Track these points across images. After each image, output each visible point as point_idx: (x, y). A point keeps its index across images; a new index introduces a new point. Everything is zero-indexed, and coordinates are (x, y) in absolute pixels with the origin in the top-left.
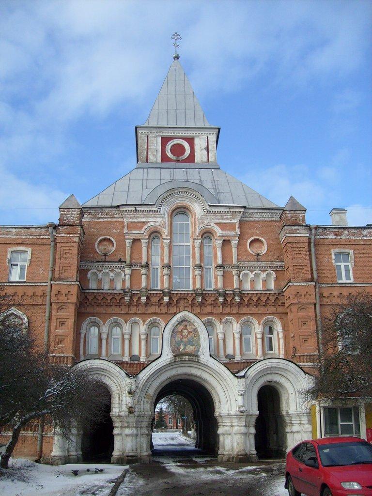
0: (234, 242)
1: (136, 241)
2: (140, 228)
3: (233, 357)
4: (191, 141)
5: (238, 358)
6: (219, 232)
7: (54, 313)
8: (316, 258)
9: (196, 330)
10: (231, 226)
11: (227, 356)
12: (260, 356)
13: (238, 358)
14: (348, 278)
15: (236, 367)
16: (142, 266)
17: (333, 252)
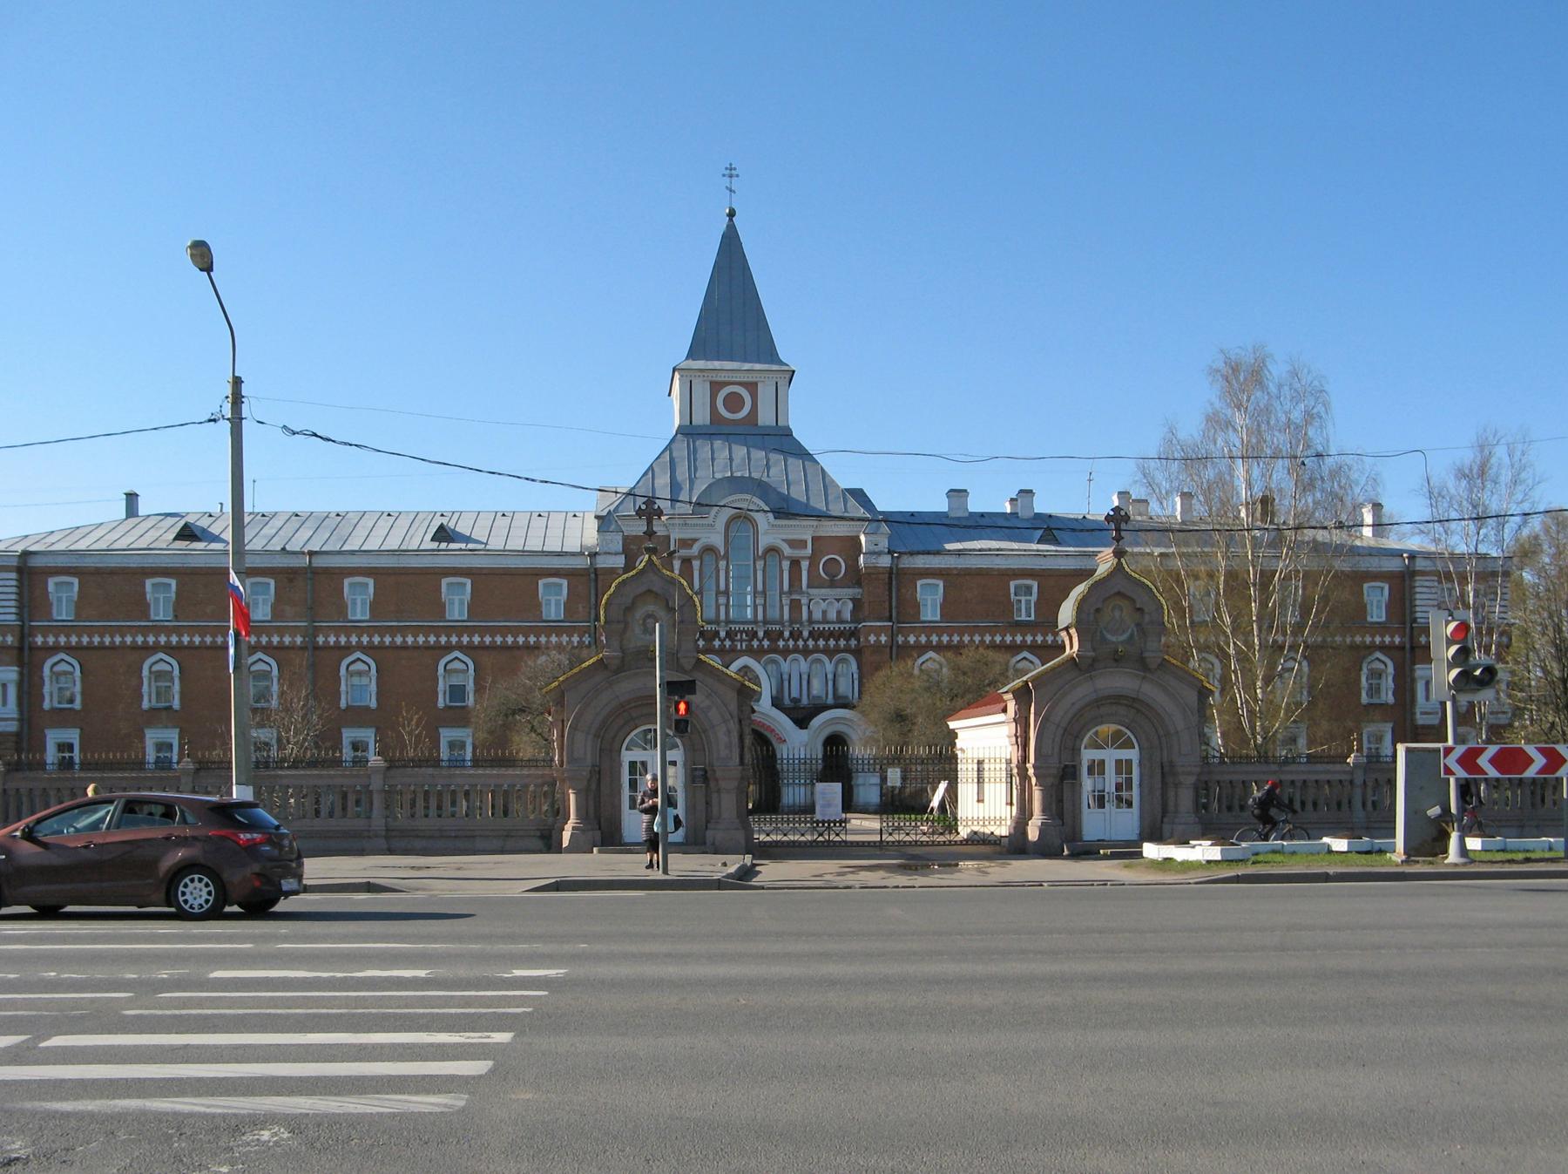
0: (805, 565)
1: (687, 562)
2: (691, 546)
3: (799, 700)
4: (752, 387)
5: (805, 701)
6: (787, 551)
8: (898, 590)
10: (803, 544)
11: (796, 701)
12: (830, 700)
13: (805, 701)
14: (934, 614)
15: (802, 717)
17: (919, 583)
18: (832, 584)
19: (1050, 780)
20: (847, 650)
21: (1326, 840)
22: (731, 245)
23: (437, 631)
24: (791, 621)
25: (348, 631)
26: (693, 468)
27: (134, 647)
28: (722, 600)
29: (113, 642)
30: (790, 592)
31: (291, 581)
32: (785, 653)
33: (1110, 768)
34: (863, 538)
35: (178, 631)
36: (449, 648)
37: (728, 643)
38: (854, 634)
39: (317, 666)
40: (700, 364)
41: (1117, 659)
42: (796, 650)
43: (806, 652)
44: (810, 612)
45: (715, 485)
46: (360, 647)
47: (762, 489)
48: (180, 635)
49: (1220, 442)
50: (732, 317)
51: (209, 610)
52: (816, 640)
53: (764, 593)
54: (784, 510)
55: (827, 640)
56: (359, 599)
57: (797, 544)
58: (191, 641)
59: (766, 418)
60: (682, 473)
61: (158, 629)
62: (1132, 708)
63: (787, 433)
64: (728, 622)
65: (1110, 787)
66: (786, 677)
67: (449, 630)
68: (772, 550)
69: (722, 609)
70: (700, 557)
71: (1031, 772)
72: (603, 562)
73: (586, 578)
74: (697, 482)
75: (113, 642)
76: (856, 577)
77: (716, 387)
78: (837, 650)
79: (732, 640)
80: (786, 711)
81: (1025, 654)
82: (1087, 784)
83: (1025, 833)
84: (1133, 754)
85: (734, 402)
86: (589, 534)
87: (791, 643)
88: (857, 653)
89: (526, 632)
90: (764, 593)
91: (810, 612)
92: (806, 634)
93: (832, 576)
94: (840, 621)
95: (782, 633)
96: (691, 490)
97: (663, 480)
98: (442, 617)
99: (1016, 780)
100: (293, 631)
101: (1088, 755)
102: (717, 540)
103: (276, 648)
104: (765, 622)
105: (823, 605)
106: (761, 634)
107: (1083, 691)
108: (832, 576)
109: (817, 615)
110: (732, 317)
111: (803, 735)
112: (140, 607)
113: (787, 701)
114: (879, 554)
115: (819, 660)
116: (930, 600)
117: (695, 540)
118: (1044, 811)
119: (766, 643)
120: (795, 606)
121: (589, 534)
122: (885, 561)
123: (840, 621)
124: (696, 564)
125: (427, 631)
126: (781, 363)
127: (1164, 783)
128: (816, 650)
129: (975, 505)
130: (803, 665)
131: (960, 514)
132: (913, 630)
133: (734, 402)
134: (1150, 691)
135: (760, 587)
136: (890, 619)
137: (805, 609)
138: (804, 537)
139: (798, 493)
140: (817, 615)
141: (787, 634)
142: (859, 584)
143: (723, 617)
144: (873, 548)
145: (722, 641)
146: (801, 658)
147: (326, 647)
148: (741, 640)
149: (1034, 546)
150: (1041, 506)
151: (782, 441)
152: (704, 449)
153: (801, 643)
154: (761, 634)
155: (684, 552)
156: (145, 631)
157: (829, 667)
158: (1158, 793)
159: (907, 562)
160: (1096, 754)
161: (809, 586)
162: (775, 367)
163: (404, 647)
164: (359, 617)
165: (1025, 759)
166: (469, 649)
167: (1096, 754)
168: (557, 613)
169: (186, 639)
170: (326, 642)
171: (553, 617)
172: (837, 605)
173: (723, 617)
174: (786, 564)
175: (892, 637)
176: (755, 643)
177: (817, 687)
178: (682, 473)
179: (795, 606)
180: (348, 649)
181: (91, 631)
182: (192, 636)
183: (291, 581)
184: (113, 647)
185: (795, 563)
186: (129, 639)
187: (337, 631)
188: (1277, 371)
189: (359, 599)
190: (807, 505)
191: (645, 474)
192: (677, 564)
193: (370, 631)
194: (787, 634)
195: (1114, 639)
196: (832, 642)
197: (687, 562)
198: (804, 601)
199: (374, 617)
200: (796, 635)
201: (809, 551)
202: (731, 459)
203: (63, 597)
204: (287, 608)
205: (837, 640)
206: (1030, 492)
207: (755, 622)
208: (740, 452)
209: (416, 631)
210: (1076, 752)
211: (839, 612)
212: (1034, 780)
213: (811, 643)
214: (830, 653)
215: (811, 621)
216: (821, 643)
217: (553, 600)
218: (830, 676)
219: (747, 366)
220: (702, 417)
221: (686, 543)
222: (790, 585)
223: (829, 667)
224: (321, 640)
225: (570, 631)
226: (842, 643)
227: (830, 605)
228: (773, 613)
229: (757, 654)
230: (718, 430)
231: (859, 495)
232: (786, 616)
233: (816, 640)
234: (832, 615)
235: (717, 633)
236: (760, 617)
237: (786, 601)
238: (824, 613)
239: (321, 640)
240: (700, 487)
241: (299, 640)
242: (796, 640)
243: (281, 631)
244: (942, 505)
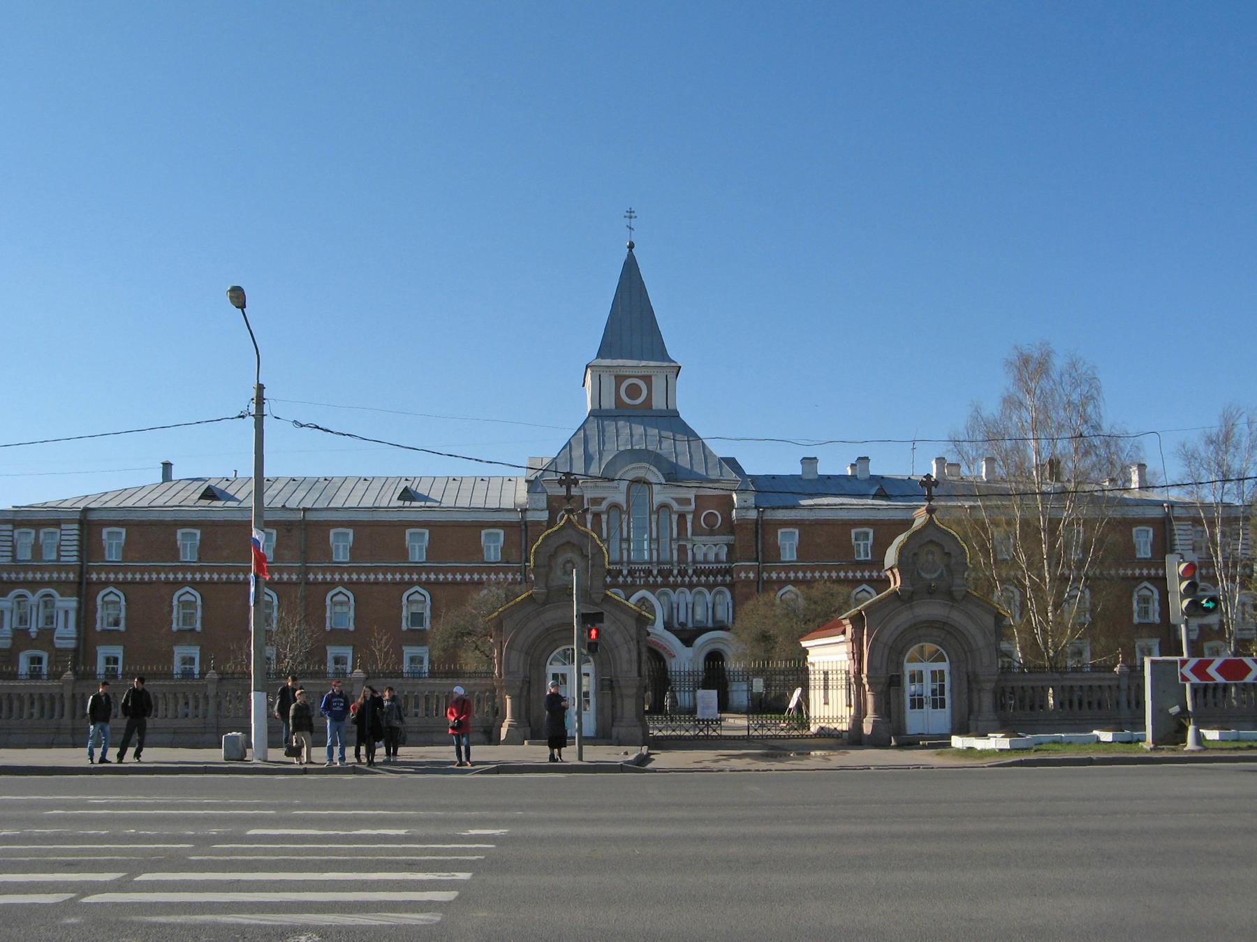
0: (689, 517)
1: (597, 516)
2: (600, 504)
4: (648, 379)
5: (690, 625)
6: (676, 506)
8: (763, 538)
10: (688, 501)
11: (681, 624)
12: (710, 624)
13: (690, 625)
17: (780, 531)
18: (712, 533)
19: (880, 688)
20: (724, 584)
22: (631, 269)
23: (402, 570)
24: (679, 562)
25: (333, 570)
26: (602, 442)
27: (167, 582)
28: (625, 546)
29: (150, 578)
30: (678, 539)
31: (289, 531)
32: (675, 587)
33: (927, 677)
34: (735, 496)
36: (411, 584)
37: (629, 579)
38: (728, 571)
39: (307, 599)
40: (607, 362)
41: (931, 592)
42: (683, 585)
43: (691, 586)
44: (694, 555)
45: (620, 454)
46: (342, 583)
47: (656, 459)
49: (1015, 418)
50: (632, 325)
52: (699, 577)
53: (658, 539)
54: (674, 475)
55: (707, 577)
56: (341, 546)
57: (684, 501)
60: (593, 447)
62: (945, 632)
63: (676, 414)
64: (629, 562)
65: (927, 692)
66: (675, 606)
67: (411, 570)
68: (664, 506)
70: (608, 512)
71: (865, 680)
72: (531, 516)
73: (519, 529)
74: (605, 454)
75: (150, 578)
76: (730, 527)
77: (619, 379)
78: (715, 584)
79: (633, 577)
80: (676, 633)
81: (864, 586)
82: (910, 688)
83: (861, 729)
84: (944, 666)
85: (633, 391)
86: (518, 494)
87: (679, 579)
88: (731, 586)
89: (471, 571)
90: (658, 539)
91: (694, 555)
92: (690, 572)
93: (711, 527)
94: (717, 561)
95: (671, 571)
96: (600, 459)
97: (578, 452)
98: (406, 559)
99: (854, 687)
100: (290, 570)
101: (909, 668)
102: (621, 498)
103: (276, 583)
104: (659, 563)
105: (704, 549)
106: (655, 572)
107: (904, 618)
108: (711, 526)
109: (700, 557)
110: (632, 325)
111: (689, 652)
113: (676, 625)
114: (747, 508)
115: (700, 593)
116: (788, 545)
117: (604, 499)
118: (876, 711)
119: (659, 579)
120: (682, 550)
121: (518, 494)
122: (753, 514)
123: (717, 561)
124: (604, 517)
125: (394, 570)
127: (970, 690)
128: (699, 584)
129: (823, 469)
130: (689, 597)
131: (811, 477)
132: (774, 568)
133: (633, 391)
134: (957, 617)
135: (654, 535)
136: (757, 560)
137: (690, 553)
138: (688, 496)
139: (684, 461)
140: (700, 557)
141: (675, 572)
142: (732, 532)
143: (625, 558)
144: (743, 504)
145: (625, 577)
146: (687, 590)
147: (315, 583)
148: (640, 577)
149: (870, 502)
150: (875, 469)
151: (671, 420)
152: (610, 427)
153: (687, 579)
154: (655, 572)
155: (595, 508)
156: (175, 569)
157: (709, 598)
158: (965, 696)
159: (770, 515)
160: (916, 667)
162: (665, 364)
163: (376, 583)
164: (341, 559)
165: (860, 671)
166: (426, 584)
167: (916, 667)
169: (207, 576)
170: (316, 578)
171: (492, 559)
172: (715, 549)
173: (625, 558)
174: (675, 517)
175: (759, 574)
176: (651, 579)
177: (700, 614)
178: (593, 447)
179: (682, 550)
180: (333, 584)
181: (134, 570)
182: (211, 574)
183: (289, 531)
184: (151, 583)
185: (682, 516)
186: (163, 576)
187: (324, 570)
188: (1059, 363)
189: (341, 546)
190: (691, 471)
191: (565, 447)
192: (589, 517)
193: (349, 570)
194: (675, 572)
195: (928, 576)
196: (711, 578)
197: (597, 516)
198: (689, 546)
199: (354, 557)
200: (683, 573)
202: (632, 435)
203: (113, 543)
205: (715, 577)
206: (867, 458)
207: (651, 562)
208: (639, 430)
209: (386, 570)
210: (900, 665)
211: (717, 555)
212: (867, 687)
213: (695, 579)
214: (710, 587)
215: (694, 562)
216: (703, 579)
217: (493, 546)
218: (710, 605)
219: (644, 363)
220: (608, 403)
221: (597, 501)
222: (679, 534)
223: (709, 598)
224: (311, 577)
225: (506, 571)
226: (719, 578)
227: (709, 549)
228: (665, 556)
229: (652, 587)
230: (622, 412)
231: (732, 463)
232: (675, 558)
233: (699, 577)
234: (712, 557)
235: (621, 571)
236: (655, 559)
237: (675, 546)
238: (705, 555)
239: (311, 577)
240: (608, 457)
242: (683, 577)
244: (797, 470)
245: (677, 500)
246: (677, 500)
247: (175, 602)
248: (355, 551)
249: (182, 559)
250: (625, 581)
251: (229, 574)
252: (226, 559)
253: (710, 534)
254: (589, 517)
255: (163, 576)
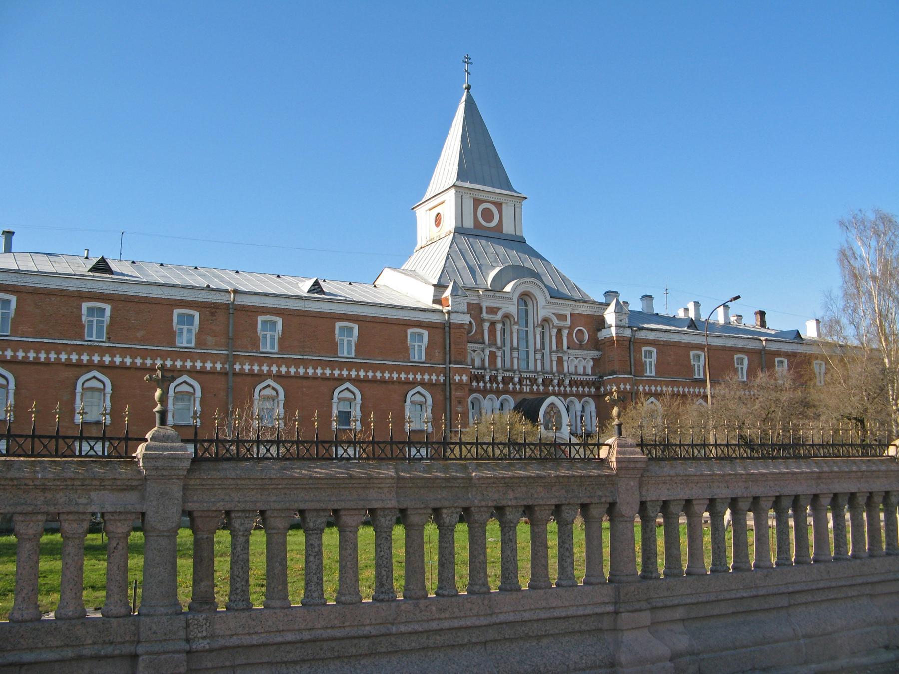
1: (493, 324)
2: (496, 313)
7: (453, 393)
9: (559, 412)
16: (499, 349)
21: (726, 523)
25: (260, 361)
27: (69, 365)
29: (48, 358)
35: (112, 352)
39: (384, 396)
48: (113, 356)
51: (140, 334)
56: (270, 335)
58: (122, 362)
59: (508, 228)
61: (92, 349)
67: (341, 365)
68: (546, 320)
69: (516, 361)
75: (48, 358)
76: (596, 344)
81: (347, 385)
87: (568, 389)
89: (399, 370)
98: (172, 343)
100: (214, 358)
103: (198, 372)
108: (581, 342)
109: (572, 370)
112: (76, 328)
117: (499, 308)
123: (585, 374)
124: (499, 326)
125: (324, 364)
126: (515, 191)
147: (242, 374)
151: (518, 242)
156: (80, 350)
161: (568, 348)
163: (306, 378)
164: (268, 350)
168: (419, 357)
169: (118, 360)
170: (242, 369)
171: (416, 360)
173: (516, 367)
180: (261, 377)
181: (27, 347)
182: (69, 354)
184: (48, 364)
185: (560, 331)
186: (64, 357)
187: (252, 360)
189: (270, 335)
193: (279, 362)
197: (493, 324)
199: (282, 349)
201: (569, 322)
204: (209, 338)
209: (316, 364)
221: (492, 310)
223: (578, 407)
224: (237, 367)
225: (430, 371)
232: (555, 369)
238: (584, 368)
239: (237, 367)
241: (219, 366)
243: (204, 358)
245: (556, 315)
246: (556, 315)
247: (79, 389)
248: (284, 342)
249: (178, 345)
250: (515, 388)
251: (38, 352)
252: (142, 341)
253: (580, 349)
254: (487, 325)
255: (64, 357)
